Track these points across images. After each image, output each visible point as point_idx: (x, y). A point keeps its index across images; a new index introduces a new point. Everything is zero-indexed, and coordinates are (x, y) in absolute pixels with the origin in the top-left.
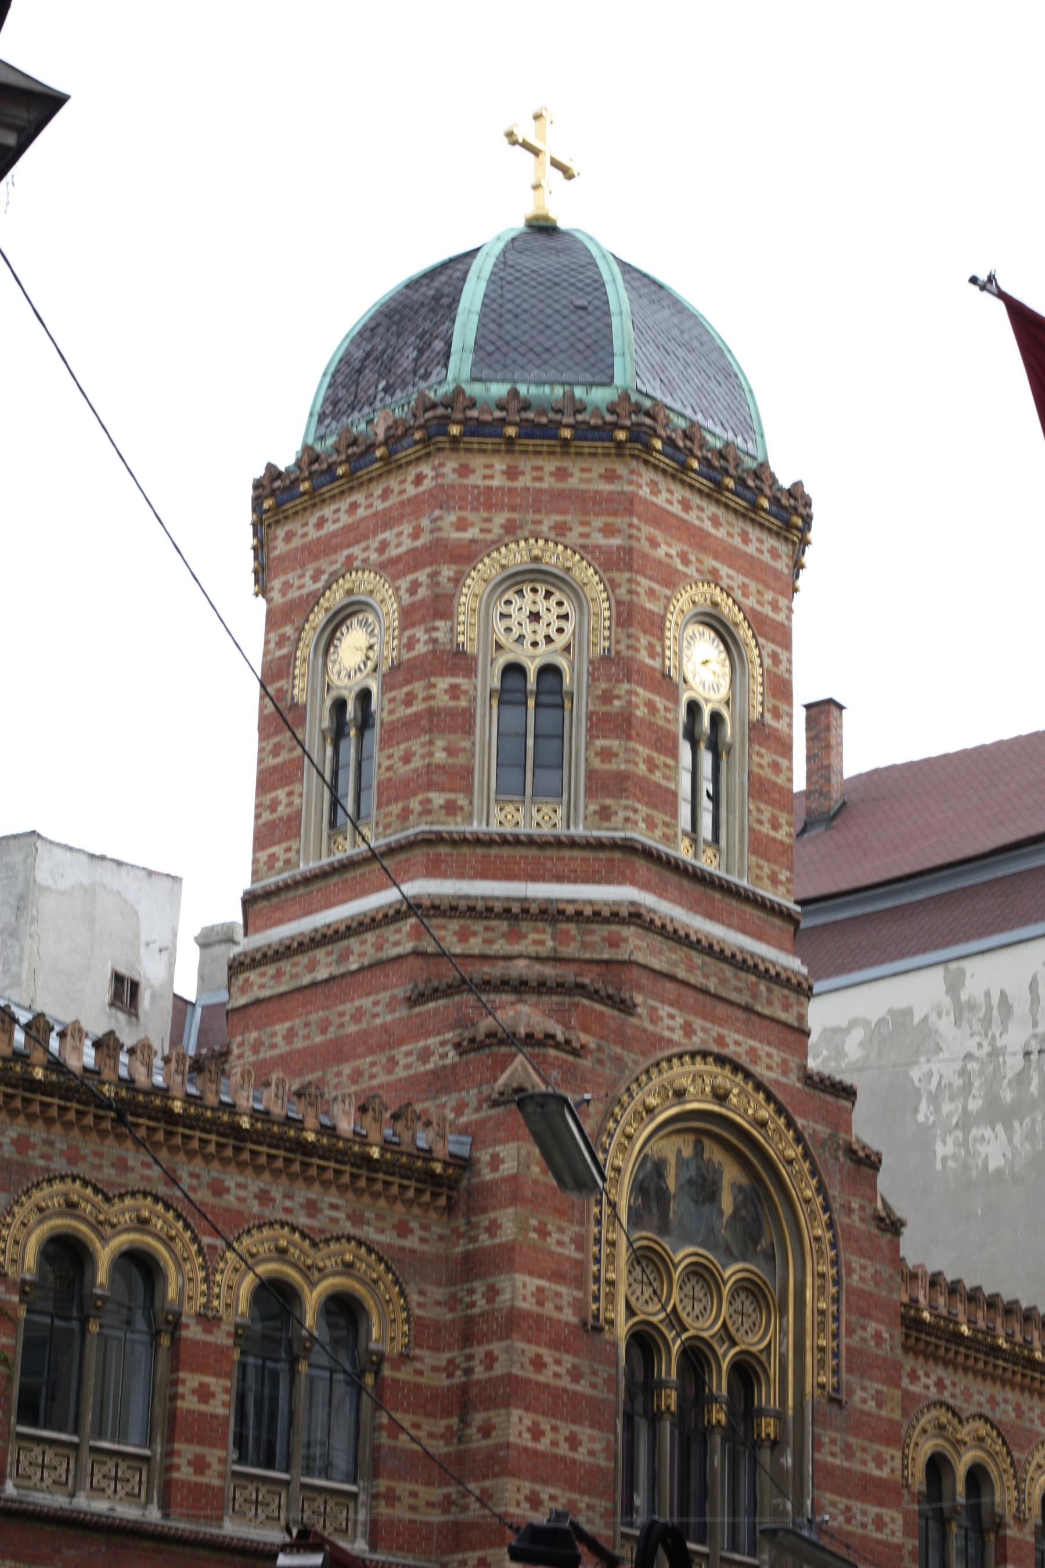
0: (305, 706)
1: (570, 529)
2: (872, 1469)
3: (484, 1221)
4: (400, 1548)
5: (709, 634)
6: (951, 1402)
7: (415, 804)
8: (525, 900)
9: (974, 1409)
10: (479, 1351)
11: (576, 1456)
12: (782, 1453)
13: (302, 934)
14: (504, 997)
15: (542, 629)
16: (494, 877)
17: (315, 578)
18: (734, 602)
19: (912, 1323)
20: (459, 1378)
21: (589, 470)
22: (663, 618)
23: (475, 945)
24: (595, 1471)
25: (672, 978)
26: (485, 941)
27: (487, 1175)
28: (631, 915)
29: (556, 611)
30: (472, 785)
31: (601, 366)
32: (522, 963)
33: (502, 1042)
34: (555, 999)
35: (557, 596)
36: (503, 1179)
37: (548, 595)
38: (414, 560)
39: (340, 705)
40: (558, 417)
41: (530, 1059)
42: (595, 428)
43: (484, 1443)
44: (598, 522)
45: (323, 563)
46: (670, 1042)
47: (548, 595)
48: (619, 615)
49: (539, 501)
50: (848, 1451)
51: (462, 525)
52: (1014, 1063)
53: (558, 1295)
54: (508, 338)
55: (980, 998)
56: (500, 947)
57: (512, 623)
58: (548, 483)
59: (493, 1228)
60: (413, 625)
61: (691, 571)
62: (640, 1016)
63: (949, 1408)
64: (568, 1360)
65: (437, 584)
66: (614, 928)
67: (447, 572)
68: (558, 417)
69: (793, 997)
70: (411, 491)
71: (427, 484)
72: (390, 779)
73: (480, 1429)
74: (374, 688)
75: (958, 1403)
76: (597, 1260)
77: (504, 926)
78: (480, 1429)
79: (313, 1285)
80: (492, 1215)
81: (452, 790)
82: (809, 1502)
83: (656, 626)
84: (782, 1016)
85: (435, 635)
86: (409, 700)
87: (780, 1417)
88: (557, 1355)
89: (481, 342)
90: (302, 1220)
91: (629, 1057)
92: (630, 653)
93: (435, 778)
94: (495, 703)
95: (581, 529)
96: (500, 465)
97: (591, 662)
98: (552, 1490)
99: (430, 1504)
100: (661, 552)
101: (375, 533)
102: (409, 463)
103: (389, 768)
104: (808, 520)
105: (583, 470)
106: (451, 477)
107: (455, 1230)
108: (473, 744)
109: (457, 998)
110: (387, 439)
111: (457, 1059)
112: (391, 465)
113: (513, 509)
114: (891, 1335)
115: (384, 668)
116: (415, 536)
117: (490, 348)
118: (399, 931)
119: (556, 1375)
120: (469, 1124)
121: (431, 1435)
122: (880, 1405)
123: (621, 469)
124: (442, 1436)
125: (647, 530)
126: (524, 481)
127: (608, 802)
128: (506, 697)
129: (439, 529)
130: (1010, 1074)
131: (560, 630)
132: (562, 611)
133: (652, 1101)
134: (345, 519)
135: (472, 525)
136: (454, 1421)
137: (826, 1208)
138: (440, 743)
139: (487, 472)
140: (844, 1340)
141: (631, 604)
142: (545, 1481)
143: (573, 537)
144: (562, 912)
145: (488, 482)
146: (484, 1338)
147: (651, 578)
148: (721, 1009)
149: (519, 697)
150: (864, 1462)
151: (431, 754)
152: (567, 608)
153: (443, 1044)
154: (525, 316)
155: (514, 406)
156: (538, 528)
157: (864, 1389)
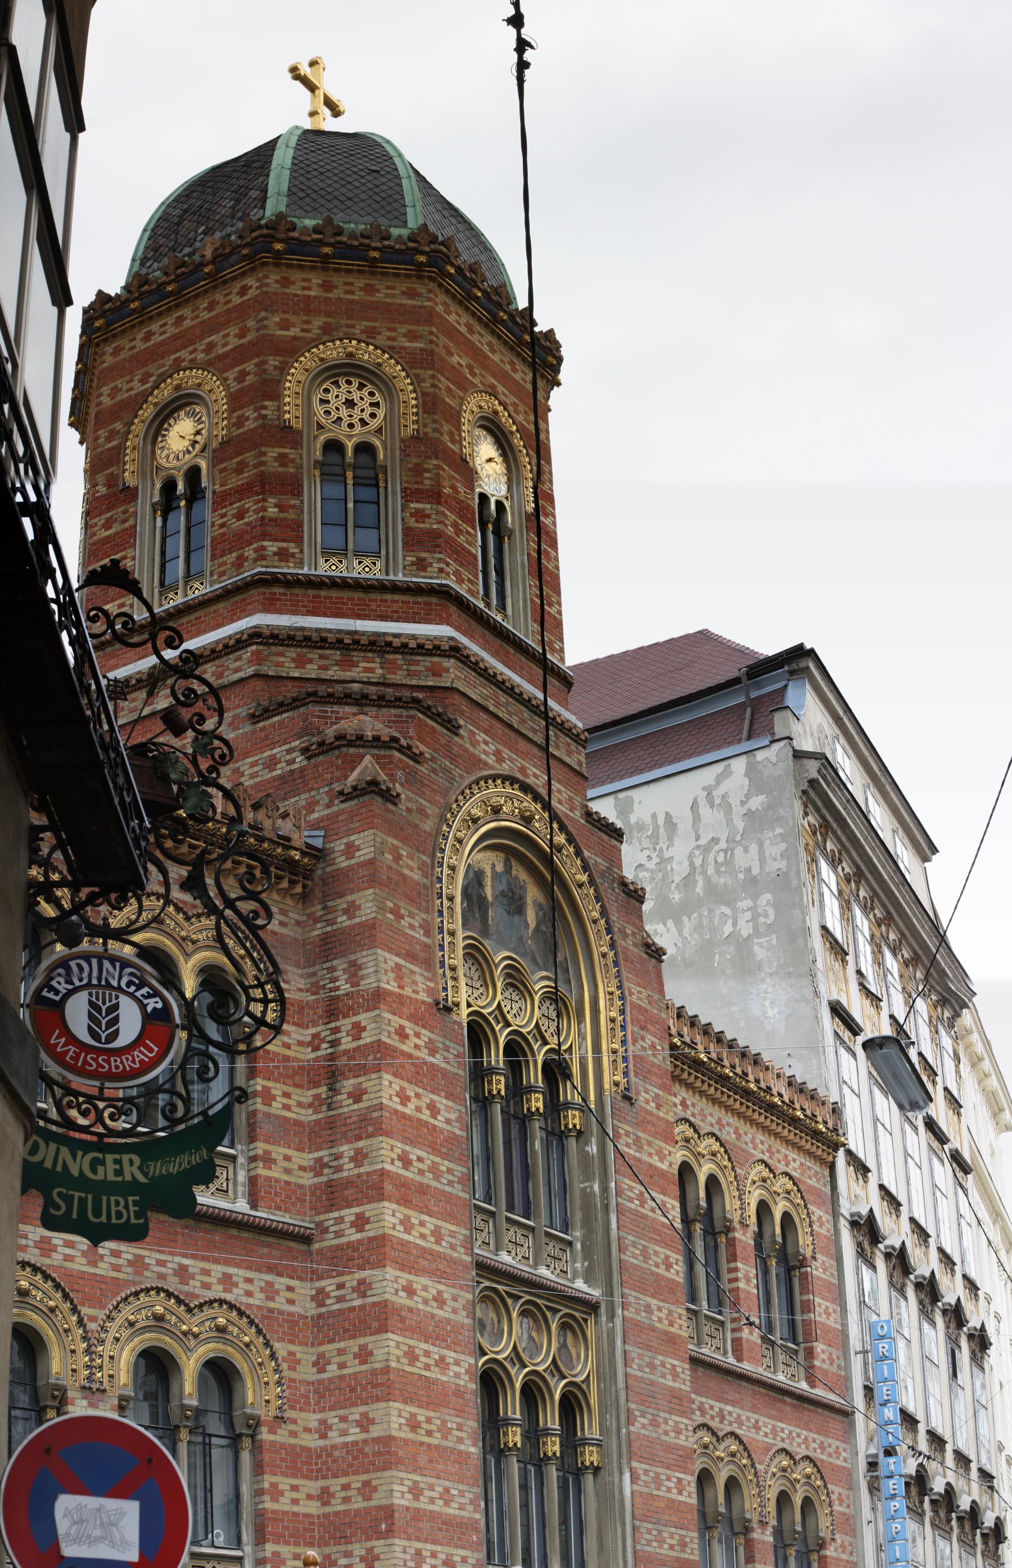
0: (137, 488)
1: (379, 333)
2: (655, 1161)
3: (342, 904)
4: (279, 1208)
5: (490, 439)
6: (692, 1119)
7: (250, 552)
8: (356, 632)
9: (709, 1129)
10: (346, 1024)
11: (436, 1122)
12: (587, 1143)
13: (140, 672)
14: (347, 709)
16: (324, 615)
17: (143, 381)
18: (510, 416)
20: (325, 1050)
21: (393, 288)
22: (459, 413)
23: (311, 671)
24: (452, 1139)
25: (485, 709)
26: (320, 668)
27: (343, 863)
28: (451, 648)
29: (368, 400)
30: (302, 537)
31: (396, 213)
32: (356, 685)
33: (351, 744)
34: (393, 711)
35: (369, 388)
36: (360, 865)
37: (361, 387)
38: (241, 354)
39: (169, 486)
40: (368, 241)
41: (377, 758)
42: (399, 252)
43: (355, 1107)
44: (403, 329)
45: (151, 368)
46: (486, 764)
47: (361, 387)
48: (425, 404)
51: (285, 325)
52: (680, 869)
54: (316, 188)
55: (648, 820)
56: (334, 673)
57: (332, 406)
59: (351, 910)
60: (242, 407)
61: (476, 381)
62: (462, 737)
63: (691, 1125)
65: (265, 371)
66: (436, 659)
67: (273, 362)
68: (368, 241)
69: (574, 746)
70: (236, 300)
71: (252, 293)
72: (224, 534)
73: (350, 1095)
74: (203, 465)
76: (442, 947)
77: (337, 655)
78: (350, 1095)
79: (188, 955)
80: (350, 898)
81: (284, 541)
82: (613, 1185)
83: (454, 418)
84: (568, 760)
85: (264, 412)
86: (240, 469)
87: (584, 1109)
88: (417, 1029)
89: (294, 189)
91: (457, 772)
92: (436, 435)
93: (269, 529)
94: (317, 473)
95: (388, 334)
96: (316, 280)
97: (402, 441)
98: (420, 1153)
99: (302, 1168)
100: (455, 359)
101: (202, 338)
102: (234, 278)
103: (222, 526)
104: (560, 360)
105: (388, 287)
106: (275, 287)
107: (311, 916)
108: (302, 502)
109: (302, 710)
110: (215, 258)
111: (305, 763)
112: (217, 281)
113: (329, 314)
115: (215, 445)
116: (241, 335)
117: (301, 194)
118: (239, 659)
119: (417, 1047)
120: (321, 819)
121: (300, 1104)
122: (658, 1107)
123: (421, 289)
124: (310, 1105)
125: (443, 340)
127: (423, 555)
128: (327, 469)
129: (265, 327)
130: (677, 879)
131: (373, 416)
132: (374, 400)
133: (476, 812)
134: (171, 330)
135: (294, 325)
136: (323, 1090)
137: (609, 931)
138: (273, 500)
139: (305, 284)
140: (631, 1048)
141: (435, 395)
142: (413, 1143)
143: (381, 340)
144: (389, 644)
145: (306, 292)
146: (351, 1011)
147: (448, 379)
148: (522, 744)
149: (338, 470)
150: (650, 1155)
151: (264, 509)
152: (378, 397)
153: (289, 751)
154: (328, 174)
155: (329, 231)
156: (352, 331)
157: (646, 1092)
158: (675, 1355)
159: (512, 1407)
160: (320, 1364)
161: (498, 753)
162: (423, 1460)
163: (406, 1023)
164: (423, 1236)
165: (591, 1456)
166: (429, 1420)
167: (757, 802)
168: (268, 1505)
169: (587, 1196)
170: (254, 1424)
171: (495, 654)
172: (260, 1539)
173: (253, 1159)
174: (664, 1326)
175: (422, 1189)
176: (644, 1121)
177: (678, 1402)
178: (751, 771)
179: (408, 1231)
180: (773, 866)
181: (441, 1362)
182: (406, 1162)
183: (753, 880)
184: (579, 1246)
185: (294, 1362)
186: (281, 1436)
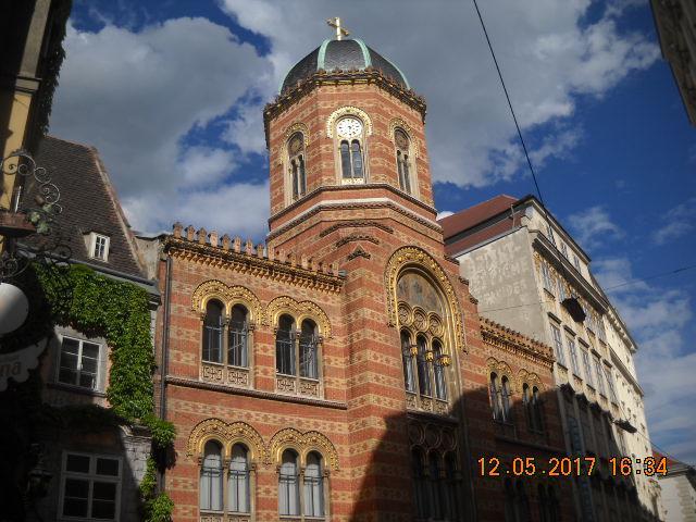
10: (354, 334)
15: (352, 130)
19: (484, 334)
27: (351, 280)
49: (347, 97)
51: (325, 105)
52: (494, 274)
58: (350, 91)
75: (497, 358)
90: (293, 296)
100: (385, 109)
114: (478, 333)
126: (342, 92)
159: (426, 462)
160: (351, 451)
161: (408, 239)
165: (458, 477)
167: (517, 249)
168: (334, 501)
169: (452, 386)
170: (327, 473)
171: (406, 206)
172: (331, 513)
173: (325, 382)
176: (474, 359)
178: (514, 237)
180: (524, 270)
182: (378, 379)
183: (519, 275)
185: (342, 450)
186: (338, 477)
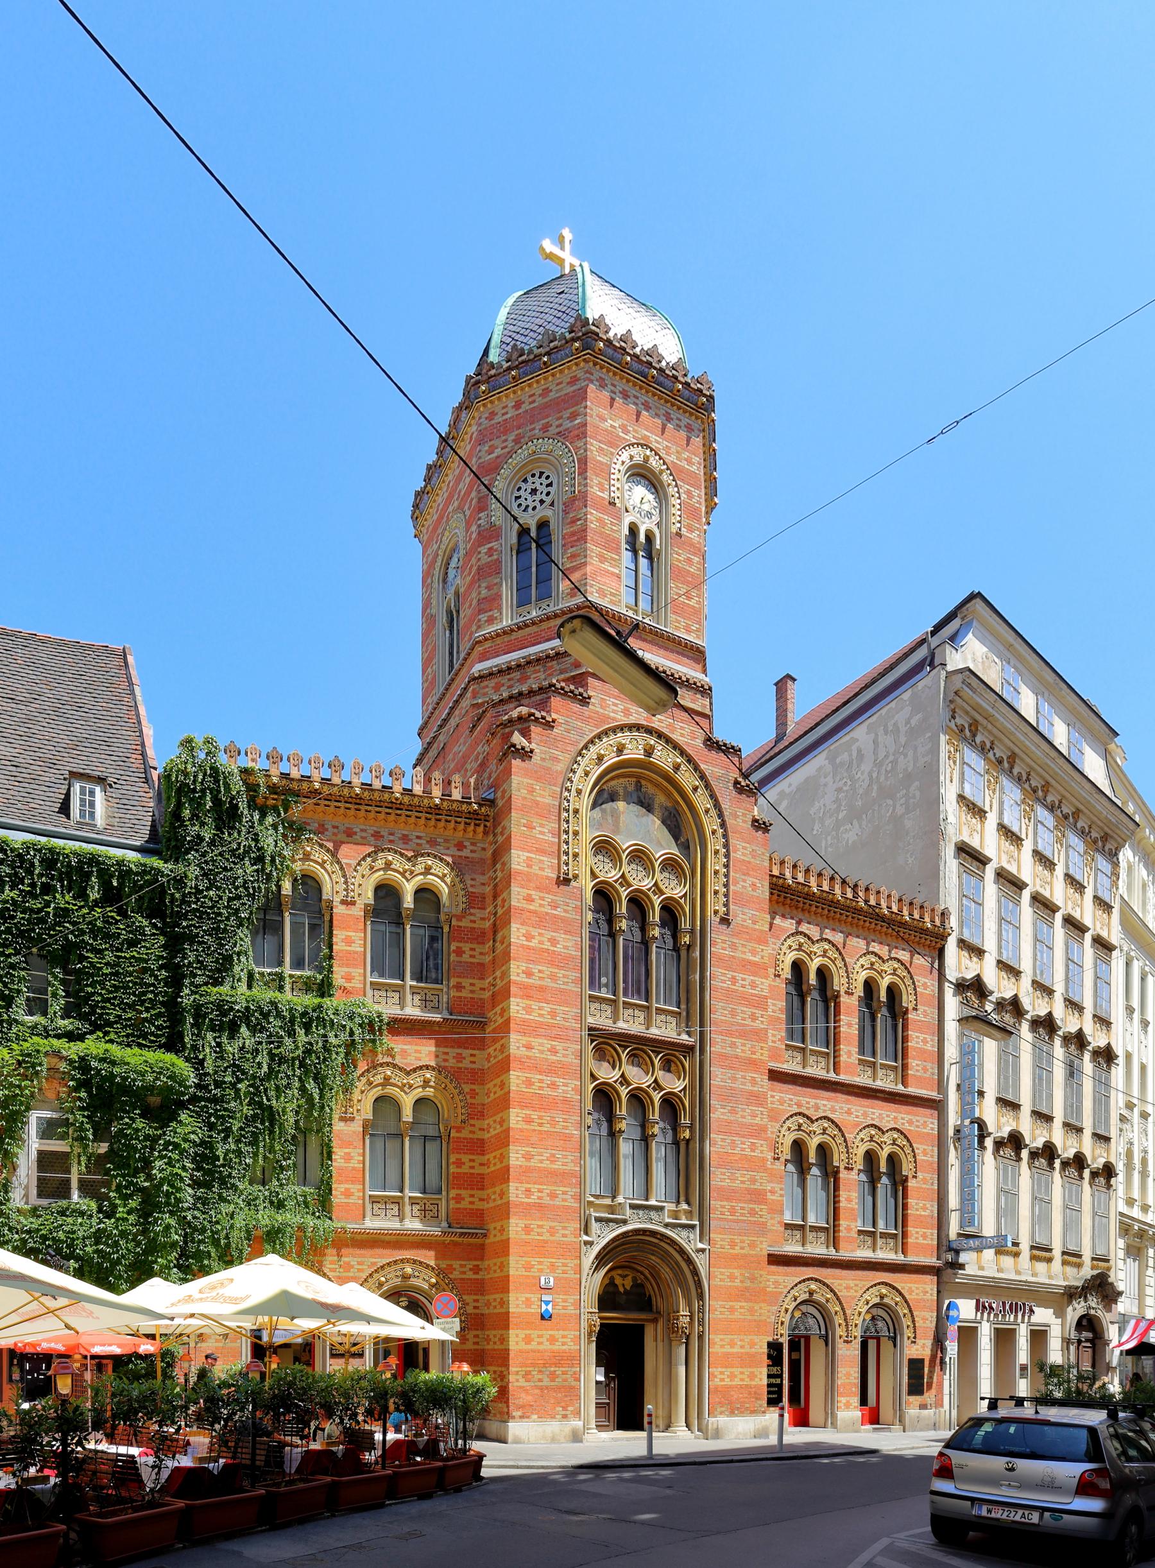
2: (749, 957)
50: (733, 946)
53: (541, 862)
64: (549, 898)
119: (541, 905)
158: (756, 1071)
162: (534, 1139)
163: (533, 892)
164: (541, 1015)
166: (540, 1118)
174: (748, 1054)
175: (542, 989)
177: (757, 1099)
179: (528, 1013)
181: (553, 1086)
182: (529, 974)
184: (684, 1014)
